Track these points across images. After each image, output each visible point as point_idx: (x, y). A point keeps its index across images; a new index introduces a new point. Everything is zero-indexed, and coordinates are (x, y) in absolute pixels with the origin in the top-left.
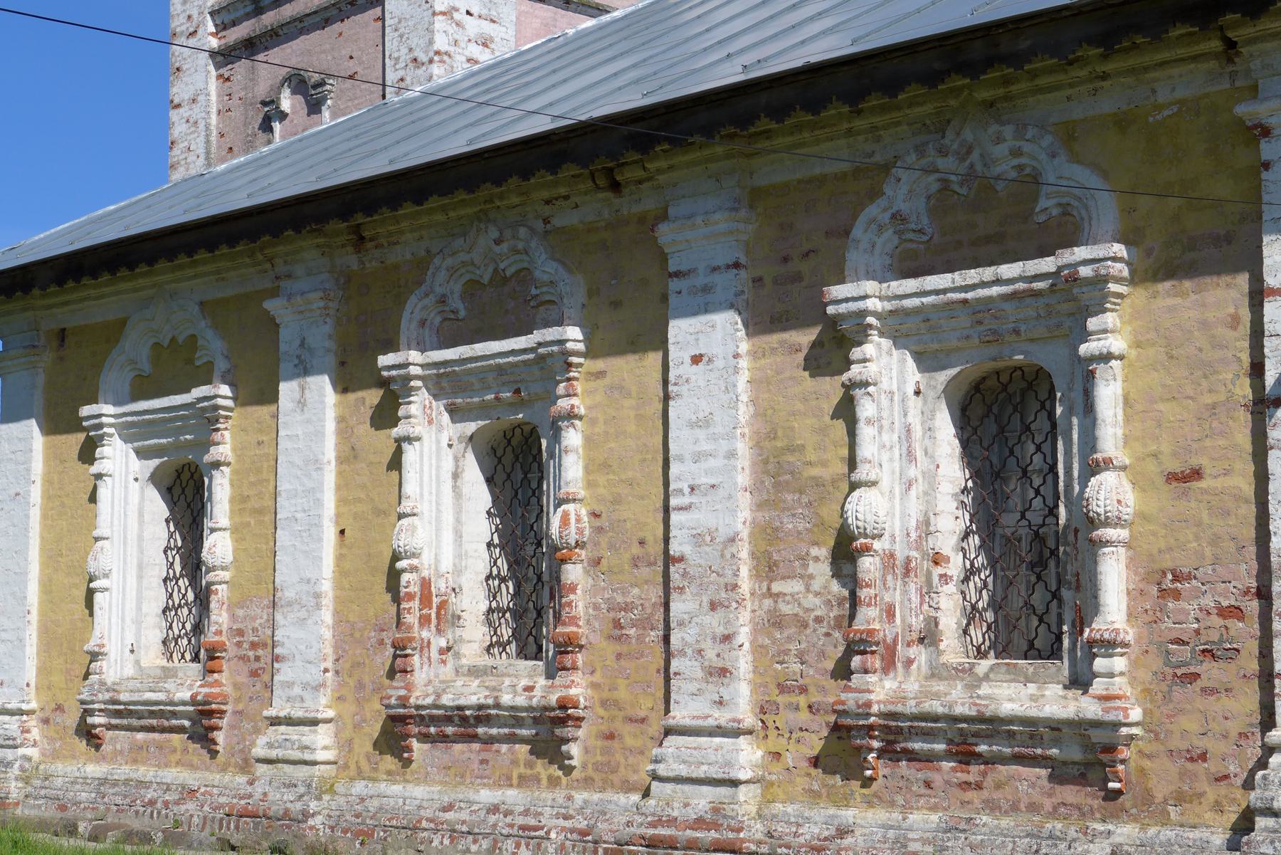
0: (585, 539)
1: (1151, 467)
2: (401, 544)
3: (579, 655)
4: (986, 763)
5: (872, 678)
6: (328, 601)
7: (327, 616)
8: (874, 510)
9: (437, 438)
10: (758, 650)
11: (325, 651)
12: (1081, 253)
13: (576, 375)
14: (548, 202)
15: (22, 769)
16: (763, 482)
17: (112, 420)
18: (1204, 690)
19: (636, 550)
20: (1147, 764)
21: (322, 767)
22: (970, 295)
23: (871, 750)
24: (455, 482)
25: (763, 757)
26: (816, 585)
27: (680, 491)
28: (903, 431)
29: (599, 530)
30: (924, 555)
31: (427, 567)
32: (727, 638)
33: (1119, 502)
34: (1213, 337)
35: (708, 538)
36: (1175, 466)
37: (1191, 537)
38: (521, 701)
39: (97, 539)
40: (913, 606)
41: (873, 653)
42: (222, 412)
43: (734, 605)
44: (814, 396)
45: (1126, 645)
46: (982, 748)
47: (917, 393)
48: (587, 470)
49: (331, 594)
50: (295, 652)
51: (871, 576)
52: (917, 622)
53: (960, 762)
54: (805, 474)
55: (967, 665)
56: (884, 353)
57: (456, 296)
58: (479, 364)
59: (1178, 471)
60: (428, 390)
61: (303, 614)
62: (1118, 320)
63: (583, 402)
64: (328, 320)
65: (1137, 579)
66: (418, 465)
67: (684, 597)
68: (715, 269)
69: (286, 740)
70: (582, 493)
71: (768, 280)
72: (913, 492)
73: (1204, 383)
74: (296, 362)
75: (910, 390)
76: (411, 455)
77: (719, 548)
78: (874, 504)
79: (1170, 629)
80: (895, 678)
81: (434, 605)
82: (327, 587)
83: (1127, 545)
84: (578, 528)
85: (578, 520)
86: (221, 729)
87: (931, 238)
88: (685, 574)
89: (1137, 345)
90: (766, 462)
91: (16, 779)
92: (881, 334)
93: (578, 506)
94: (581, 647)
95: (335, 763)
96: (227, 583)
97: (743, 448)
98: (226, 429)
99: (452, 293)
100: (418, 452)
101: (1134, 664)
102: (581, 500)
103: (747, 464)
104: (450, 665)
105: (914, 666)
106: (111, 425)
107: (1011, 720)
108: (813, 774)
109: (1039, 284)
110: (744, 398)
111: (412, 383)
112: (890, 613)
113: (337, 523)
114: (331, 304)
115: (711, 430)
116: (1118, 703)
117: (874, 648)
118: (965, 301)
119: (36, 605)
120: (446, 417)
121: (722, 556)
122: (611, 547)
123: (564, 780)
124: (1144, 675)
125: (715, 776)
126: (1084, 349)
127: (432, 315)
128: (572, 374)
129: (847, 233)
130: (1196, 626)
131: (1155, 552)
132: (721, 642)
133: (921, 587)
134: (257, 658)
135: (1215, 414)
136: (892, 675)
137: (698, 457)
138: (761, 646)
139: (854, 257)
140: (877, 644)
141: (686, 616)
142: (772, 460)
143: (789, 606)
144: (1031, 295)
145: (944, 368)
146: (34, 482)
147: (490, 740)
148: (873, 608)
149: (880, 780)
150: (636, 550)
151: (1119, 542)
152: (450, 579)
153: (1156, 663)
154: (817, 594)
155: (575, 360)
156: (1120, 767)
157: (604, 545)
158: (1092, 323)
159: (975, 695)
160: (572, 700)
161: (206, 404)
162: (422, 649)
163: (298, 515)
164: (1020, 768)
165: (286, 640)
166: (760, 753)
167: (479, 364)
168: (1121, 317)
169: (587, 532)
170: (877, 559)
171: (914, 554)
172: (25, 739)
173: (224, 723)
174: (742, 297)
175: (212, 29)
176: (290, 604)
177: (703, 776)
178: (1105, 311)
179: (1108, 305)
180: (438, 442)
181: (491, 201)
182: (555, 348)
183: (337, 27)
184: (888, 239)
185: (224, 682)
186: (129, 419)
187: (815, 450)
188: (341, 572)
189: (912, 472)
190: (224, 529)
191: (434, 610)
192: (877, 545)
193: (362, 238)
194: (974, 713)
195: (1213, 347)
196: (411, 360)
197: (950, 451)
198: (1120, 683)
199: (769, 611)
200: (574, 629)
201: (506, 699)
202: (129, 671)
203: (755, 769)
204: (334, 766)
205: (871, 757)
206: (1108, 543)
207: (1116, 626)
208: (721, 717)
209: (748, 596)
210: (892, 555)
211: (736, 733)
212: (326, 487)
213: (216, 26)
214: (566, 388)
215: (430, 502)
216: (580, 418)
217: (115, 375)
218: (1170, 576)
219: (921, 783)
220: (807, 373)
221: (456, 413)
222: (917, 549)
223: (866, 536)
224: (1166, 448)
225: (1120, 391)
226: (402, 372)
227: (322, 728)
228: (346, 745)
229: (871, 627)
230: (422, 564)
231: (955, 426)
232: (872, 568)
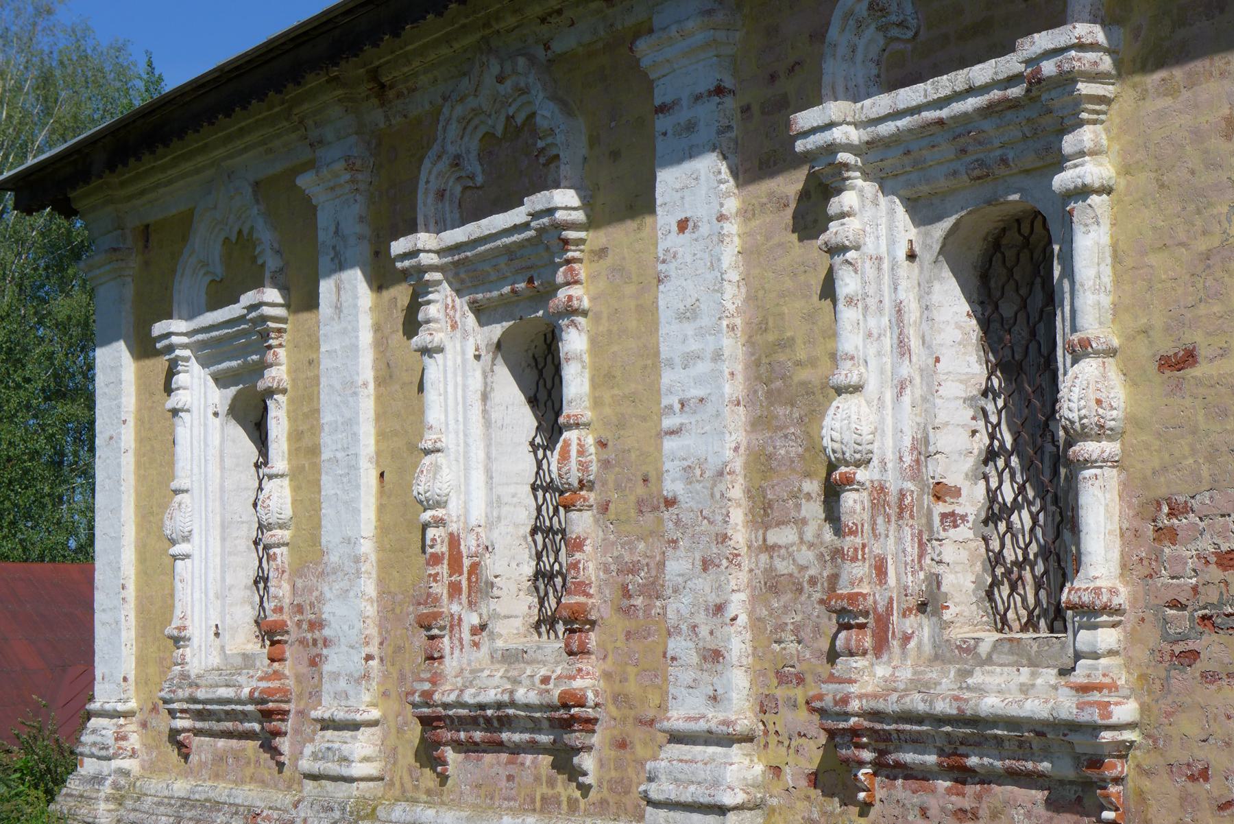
0: (592, 478)
1: (1144, 351)
2: (421, 489)
3: (592, 635)
4: (982, 782)
5: (859, 662)
6: (370, 567)
7: (369, 587)
8: (854, 426)
9: (462, 347)
10: (756, 623)
11: (367, 632)
12: (1043, 41)
13: (577, 254)
14: (543, 20)
15: (116, 786)
16: (756, 392)
17: (185, 340)
18: (1204, 675)
19: (640, 490)
20: (1146, 784)
21: (362, 785)
22: (944, 113)
23: (861, 764)
24: (485, 405)
25: (763, 773)
26: (810, 532)
27: (670, 408)
28: (894, 312)
29: (606, 464)
30: (923, 486)
31: (455, 519)
32: (719, 609)
33: (1099, 402)
34: (1206, 152)
35: (698, 472)
36: (1167, 347)
37: (1186, 450)
38: (533, 698)
39: (176, 492)
40: (909, 559)
41: (862, 626)
42: (271, 324)
43: (725, 563)
44: (802, 269)
45: (1118, 611)
46: (973, 761)
47: (911, 256)
48: (594, 385)
49: (373, 557)
50: (341, 635)
51: (857, 519)
52: (915, 582)
53: (956, 781)
54: (796, 379)
55: (972, 642)
56: (868, 202)
57: (474, 154)
58: (488, 246)
59: (1171, 353)
60: (450, 284)
61: (344, 584)
62: (1104, 136)
63: (587, 292)
64: (358, 197)
65: (1131, 513)
66: (442, 385)
67: (678, 553)
68: (698, 98)
69: (329, 749)
70: (588, 415)
71: (756, 109)
72: (907, 399)
73: (1199, 222)
75: (902, 253)
76: (434, 369)
77: (709, 485)
78: (854, 417)
79: (1167, 586)
80: (890, 660)
81: (465, 570)
82: (367, 547)
83: (1116, 464)
84: (580, 463)
85: (582, 452)
86: (285, 734)
87: (916, 34)
88: (678, 523)
89: (1126, 170)
90: (758, 364)
91: (107, 800)
92: (866, 176)
93: (584, 432)
94: (593, 623)
95: (382, 779)
96: (287, 544)
97: (733, 347)
98: (280, 345)
99: (468, 152)
100: (441, 368)
101: (1132, 638)
102: (587, 425)
103: (739, 368)
104: (484, 649)
105: (912, 644)
106: (185, 346)
107: (996, 721)
108: (813, 797)
109: (1014, 90)
110: (734, 276)
111: (427, 277)
112: (880, 569)
113: (378, 463)
114: (360, 176)
115: (699, 323)
116: (1096, 696)
117: (861, 620)
118: (940, 122)
119: (133, 577)
120: (471, 319)
121: (712, 495)
122: (618, 487)
123: (582, 802)
124: (1141, 654)
125: (701, 800)
126: (1062, 180)
127: (451, 183)
128: (570, 254)
129: (824, 36)
130: (1194, 581)
131: (1149, 473)
132: (714, 614)
133: (920, 532)
135: (1209, 267)
136: (885, 657)
137: (689, 359)
138: (759, 619)
139: (833, 69)
140: (866, 614)
141: (680, 580)
142: (764, 360)
143: (785, 563)
144: (1010, 108)
145: (939, 218)
146: (124, 422)
147: (516, 750)
148: (860, 563)
149: (878, 804)
150: (640, 490)
151: (1104, 461)
152: (483, 535)
153: (1152, 636)
154: (811, 546)
155: (571, 234)
156: (1113, 789)
157: (611, 485)
158: (1069, 143)
159: (964, 685)
160: (574, 695)
162: (452, 627)
164: (1015, 789)
165: (331, 618)
166: (759, 768)
167: (488, 246)
168: (1107, 131)
169: (594, 468)
170: (865, 494)
171: (909, 485)
172: (120, 748)
173: (288, 726)
174: (729, 135)
177: (690, 800)
178: (1081, 123)
179: (1084, 115)
180: (463, 353)
182: (546, 220)
184: (870, 40)
185: (287, 672)
186: (200, 337)
187: (805, 344)
188: (383, 529)
189: (905, 370)
190: (282, 476)
191: (465, 575)
192: (861, 475)
193: (383, 86)
194: (955, 712)
195: (1207, 167)
196: (420, 246)
197: (958, 336)
198: (1108, 667)
199: (766, 569)
200: (582, 599)
201: (522, 695)
202: (215, 660)
203: (751, 790)
204: (379, 783)
205: (863, 773)
206: (1087, 463)
207: (1098, 583)
208: (713, 719)
209: (744, 551)
210: (882, 489)
211: (727, 740)
212: (362, 417)
214: (565, 274)
215: (457, 433)
216: (584, 313)
217: (188, 285)
218: (1165, 509)
219: (917, 811)
220: (795, 236)
221: (483, 313)
222: (913, 479)
223: (847, 464)
224: (1158, 321)
225: (1105, 239)
226: (413, 262)
227: (364, 733)
228: (391, 755)
229: (856, 590)
230: (449, 515)
231: (970, 300)
232: (858, 508)
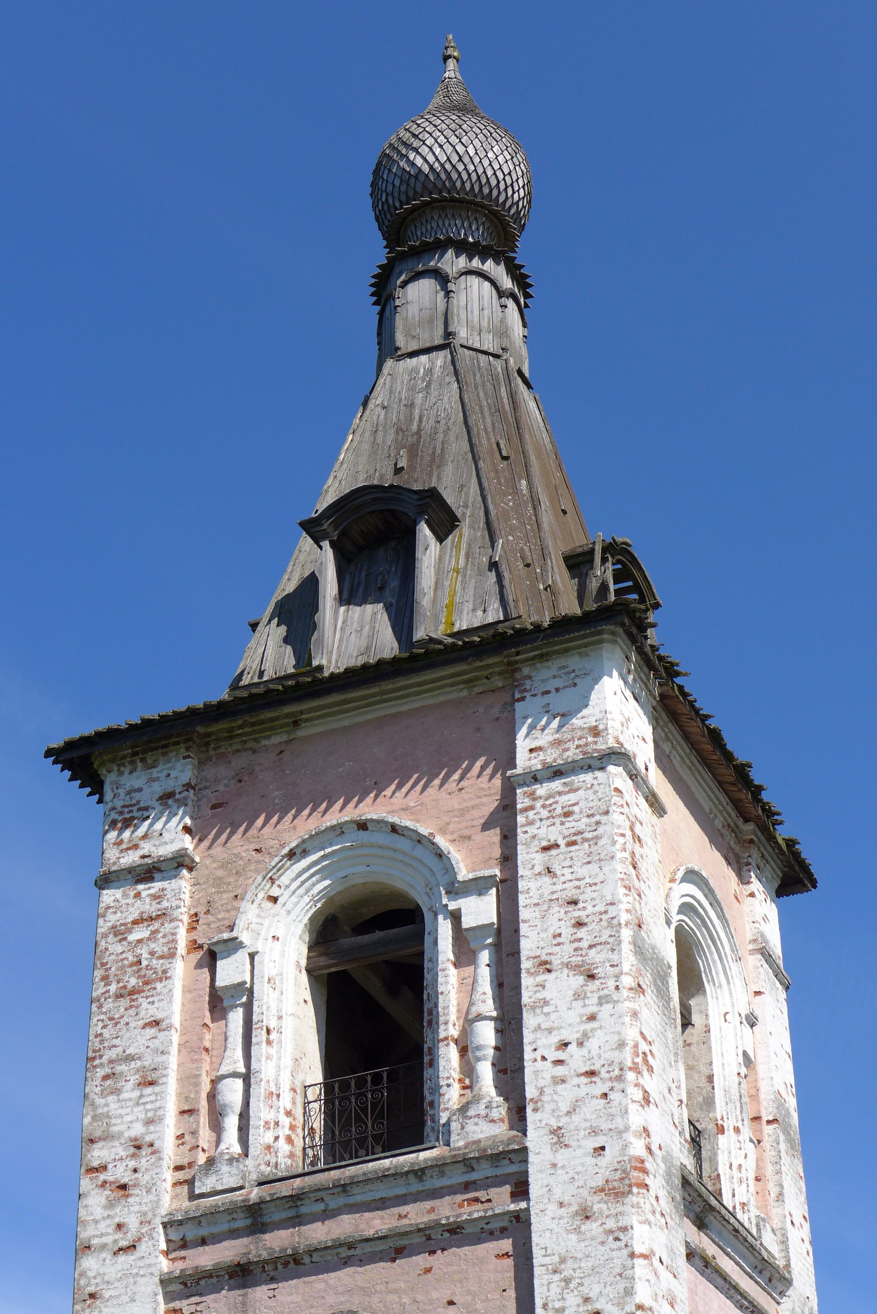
175: (163, 1246)
183: (422, 1260)
213: (168, 1241)
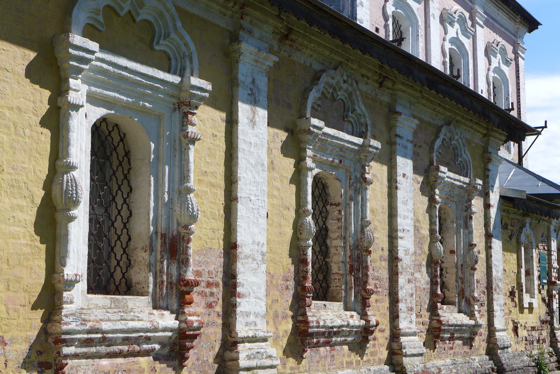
14: (362, 76)
50: (251, 291)
58: (338, 142)
61: (254, 265)
69: (258, 352)
74: (250, 92)
134: (212, 294)
141: (403, 285)
161: (199, 93)
163: (253, 198)
165: (245, 282)
167: (338, 142)
176: (247, 257)
181: (348, 61)
186: (105, 66)
